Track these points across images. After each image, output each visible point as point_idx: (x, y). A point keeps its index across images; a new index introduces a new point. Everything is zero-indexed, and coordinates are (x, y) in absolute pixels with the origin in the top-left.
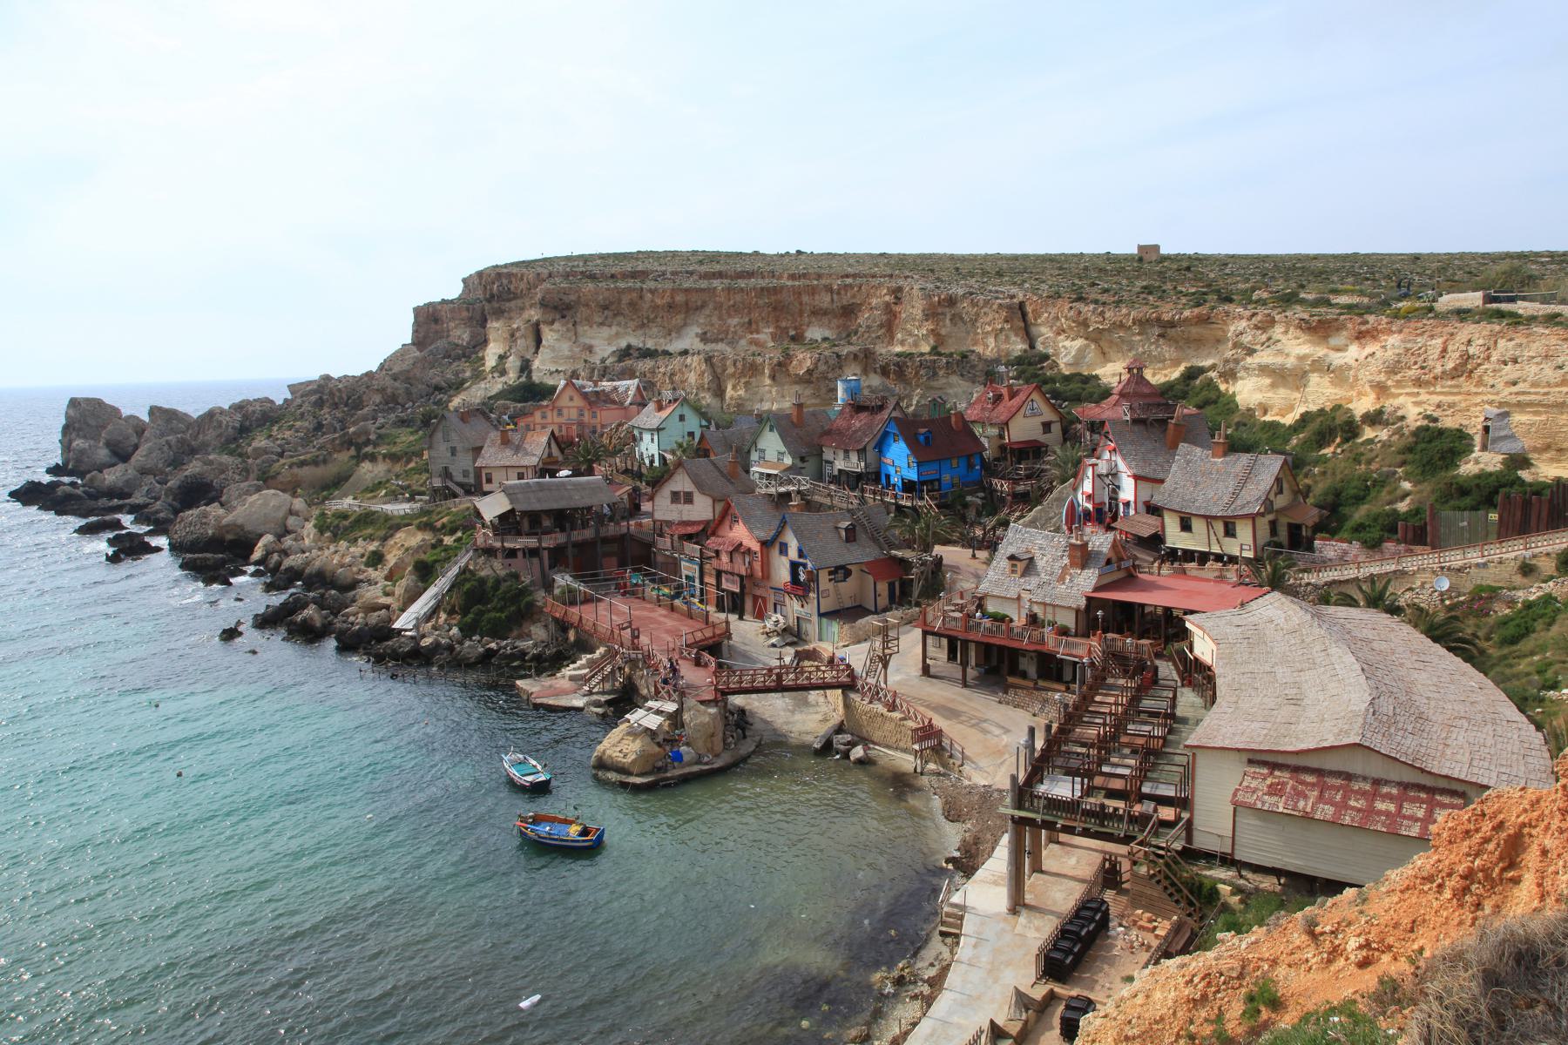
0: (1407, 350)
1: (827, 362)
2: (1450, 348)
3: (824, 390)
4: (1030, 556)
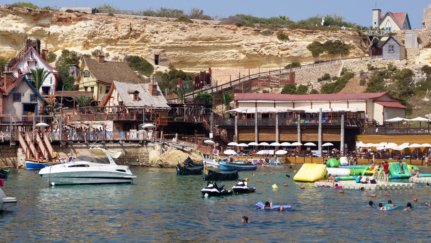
0: (97, 27)
2: (119, 27)
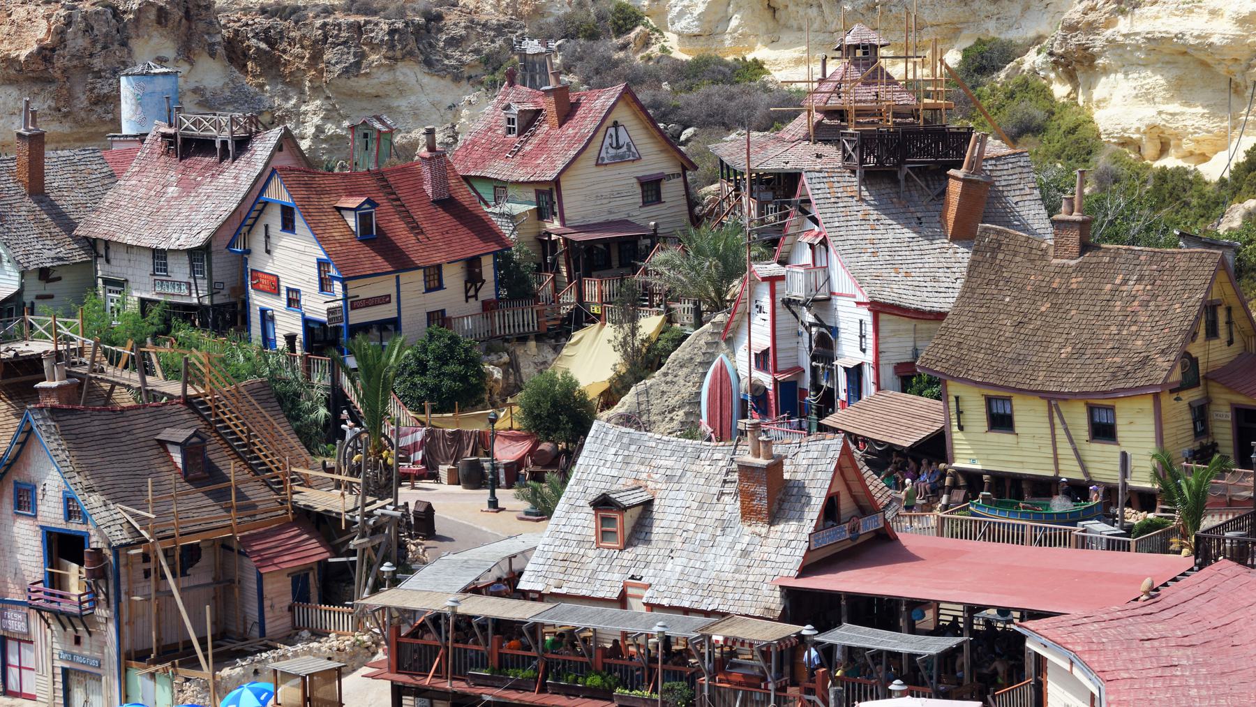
3: (82, 100)
4: (646, 497)
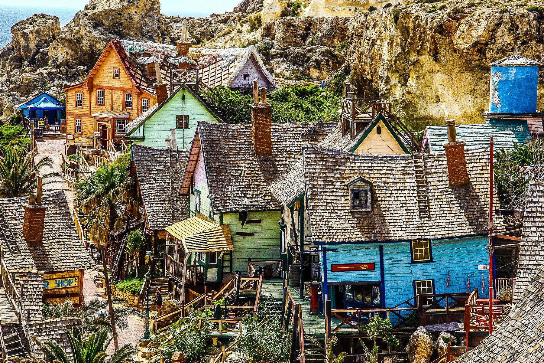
1: (514, 27)
